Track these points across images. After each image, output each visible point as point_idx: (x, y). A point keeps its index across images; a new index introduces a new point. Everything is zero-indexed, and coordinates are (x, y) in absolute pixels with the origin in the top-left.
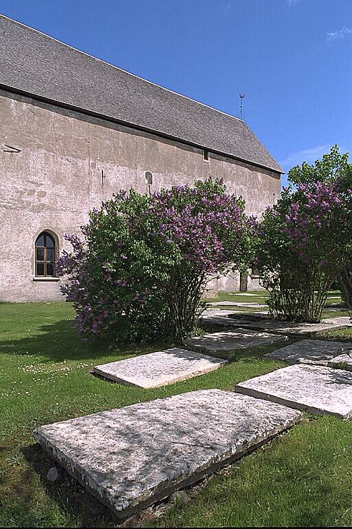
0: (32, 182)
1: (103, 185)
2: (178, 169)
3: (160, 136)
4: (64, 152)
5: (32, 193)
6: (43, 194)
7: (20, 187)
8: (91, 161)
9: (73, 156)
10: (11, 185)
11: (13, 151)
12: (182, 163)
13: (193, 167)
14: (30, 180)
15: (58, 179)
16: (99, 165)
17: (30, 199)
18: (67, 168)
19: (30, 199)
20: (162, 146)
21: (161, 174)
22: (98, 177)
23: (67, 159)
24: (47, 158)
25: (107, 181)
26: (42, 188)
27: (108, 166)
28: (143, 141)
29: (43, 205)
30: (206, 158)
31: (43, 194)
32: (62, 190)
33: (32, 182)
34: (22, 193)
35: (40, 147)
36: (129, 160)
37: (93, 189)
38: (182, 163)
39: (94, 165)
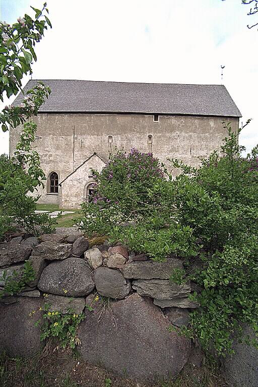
1: (82, 147)
2: (131, 130)
3: (118, 114)
4: (62, 133)
5: (46, 155)
6: (51, 155)
8: (75, 136)
9: (65, 135)
15: (58, 148)
17: (45, 158)
18: (62, 141)
19: (45, 158)
20: (120, 119)
22: (79, 144)
24: (53, 139)
25: (84, 145)
26: (50, 153)
28: (106, 119)
29: (51, 160)
30: (156, 119)
31: (51, 155)
32: (59, 152)
35: (50, 134)
36: (97, 131)
37: (76, 150)
39: (76, 138)
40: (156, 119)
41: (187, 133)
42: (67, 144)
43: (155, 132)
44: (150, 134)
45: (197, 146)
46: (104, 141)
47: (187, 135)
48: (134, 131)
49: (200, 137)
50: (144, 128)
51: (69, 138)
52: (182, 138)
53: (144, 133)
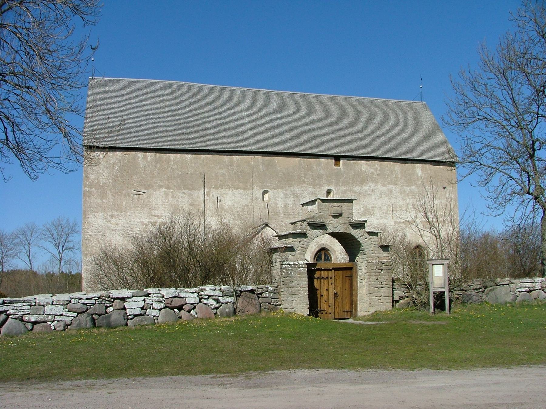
0: (155, 216)
7: (145, 221)
8: (207, 190)
9: (189, 189)
10: (139, 220)
11: (139, 193)
12: (305, 175)
13: (320, 177)
14: (153, 214)
16: (214, 193)
21: (280, 190)
22: (214, 203)
23: (184, 193)
24: (166, 194)
27: (223, 191)
30: (337, 164)
33: (155, 216)
34: (146, 225)
35: (161, 187)
38: (305, 175)
39: (208, 194)
40: (337, 164)
41: (383, 185)
42: (192, 204)
43: (337, 184)
44: (329, 188)
45: (400, 206)
46: (257, 198)
47: (384, 189)
48: (304, 183)
49: (405, 191)
50: (320, 177)
51: (195, 193)
52: (378, 194)
53: (321, 186)
